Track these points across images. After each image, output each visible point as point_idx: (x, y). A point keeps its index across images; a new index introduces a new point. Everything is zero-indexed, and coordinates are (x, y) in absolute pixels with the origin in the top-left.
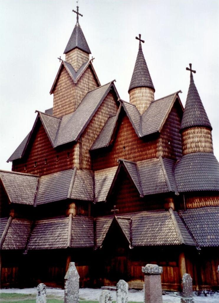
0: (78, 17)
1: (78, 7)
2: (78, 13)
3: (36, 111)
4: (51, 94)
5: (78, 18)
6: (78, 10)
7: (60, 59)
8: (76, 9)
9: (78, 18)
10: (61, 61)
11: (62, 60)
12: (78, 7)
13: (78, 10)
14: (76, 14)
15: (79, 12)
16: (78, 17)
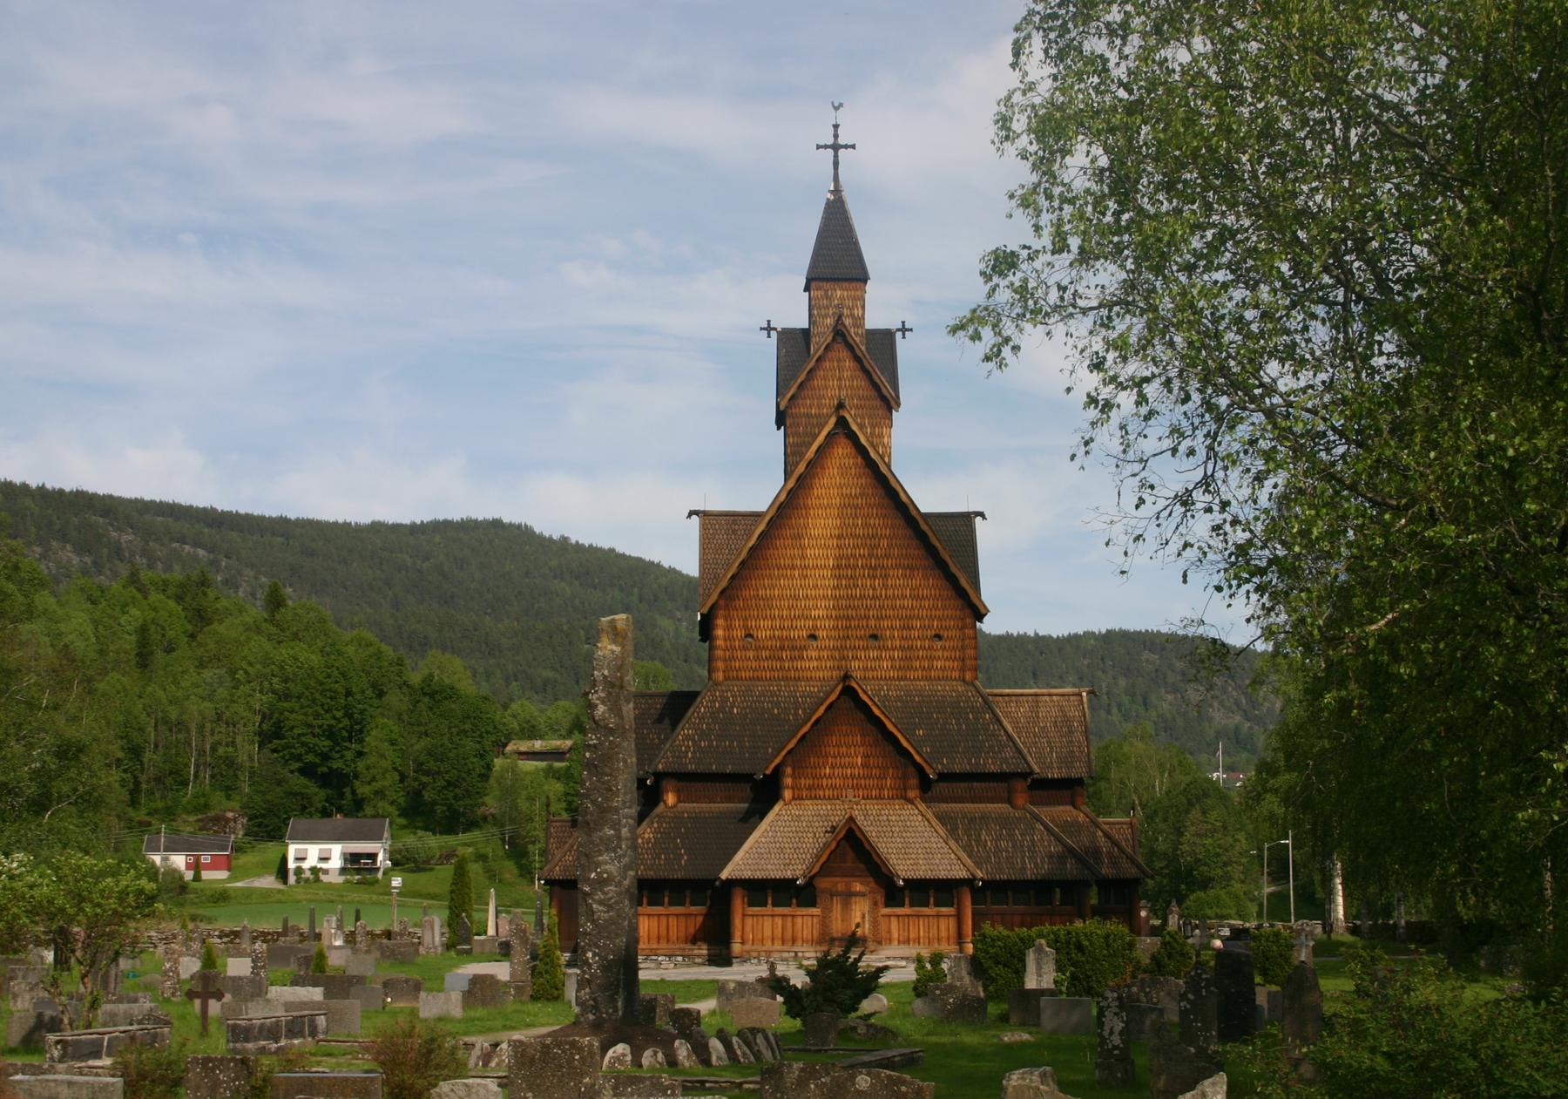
0: (836, 156)
1: (836, 127)
2: (836, 147)
3: (691, 513)
4: (779, 429)
5: (836, 164)
6: (836, 136)
7: (769, 329)
8: (832, 130)
9: (836, 164)
10: (774, 334)
11: (775, 329)
12: (836, 127)
13: (836, 136)
14: (831, 152)
15: (841, 141)
16: (836, 156)
